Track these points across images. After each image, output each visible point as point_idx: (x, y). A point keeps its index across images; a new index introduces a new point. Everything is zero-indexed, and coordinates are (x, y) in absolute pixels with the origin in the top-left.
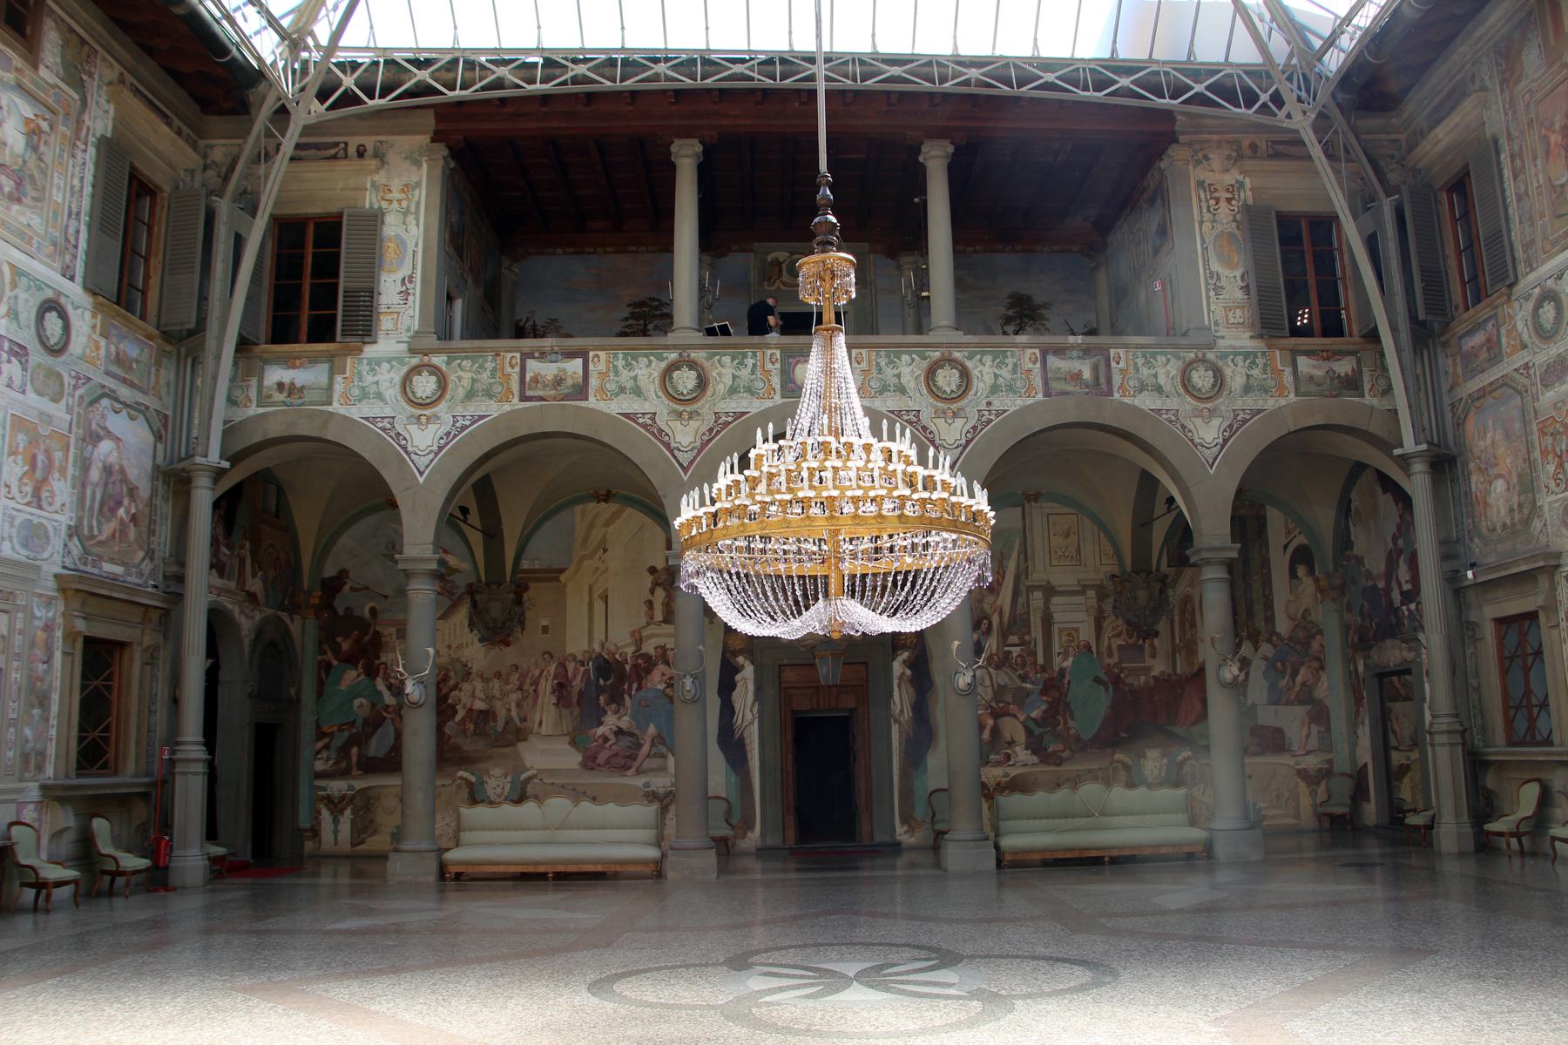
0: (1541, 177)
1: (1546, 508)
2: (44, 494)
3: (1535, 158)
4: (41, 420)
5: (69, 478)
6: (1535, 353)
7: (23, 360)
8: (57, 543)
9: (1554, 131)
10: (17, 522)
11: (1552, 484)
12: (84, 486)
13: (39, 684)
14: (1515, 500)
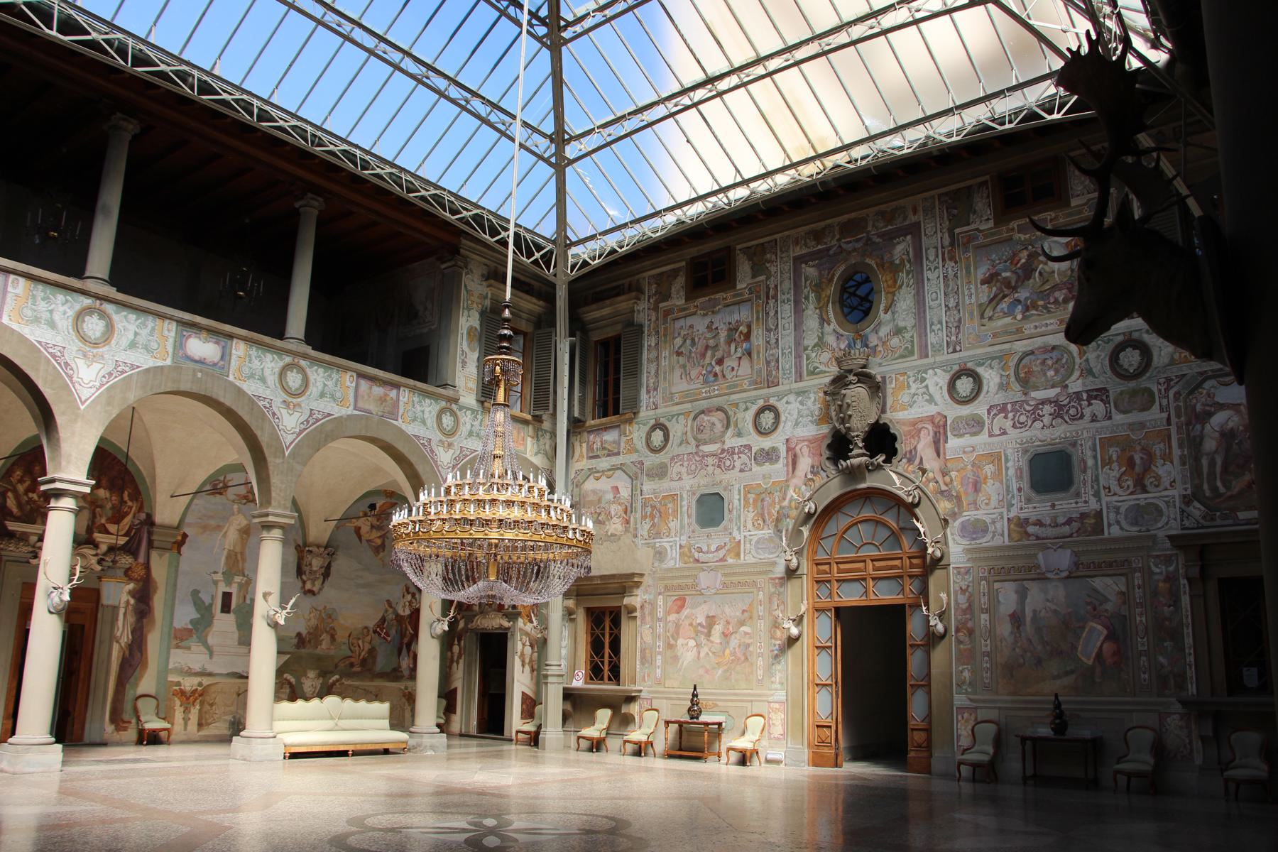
2: (1147, 482)
4: (1132, 430)
5: (1176, 460)
7: (1104, 398)
8: (1174, 513)
10: (1123, 510)
12: (1197, 459)
13: (1167, 623)
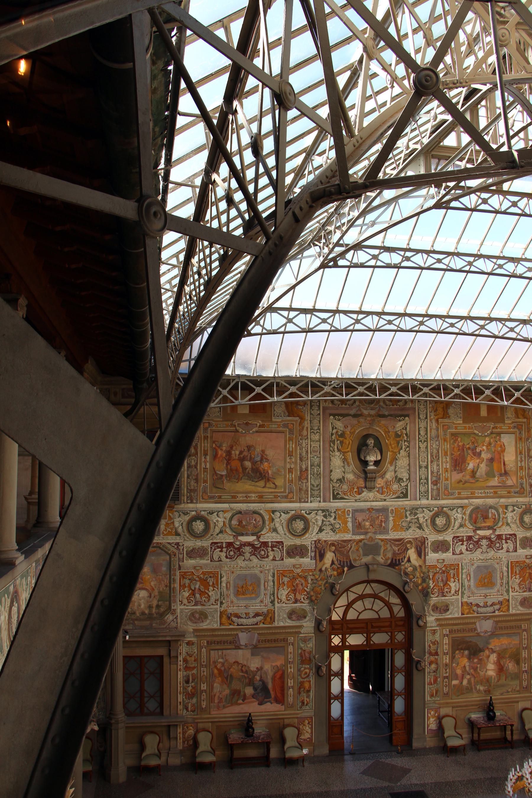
0: (208, 464)
1: (179, 611)
3: (206, 454)
6: (185, 540)
9: (222, 450)
11: (185, 601)
14: (155, 603)
